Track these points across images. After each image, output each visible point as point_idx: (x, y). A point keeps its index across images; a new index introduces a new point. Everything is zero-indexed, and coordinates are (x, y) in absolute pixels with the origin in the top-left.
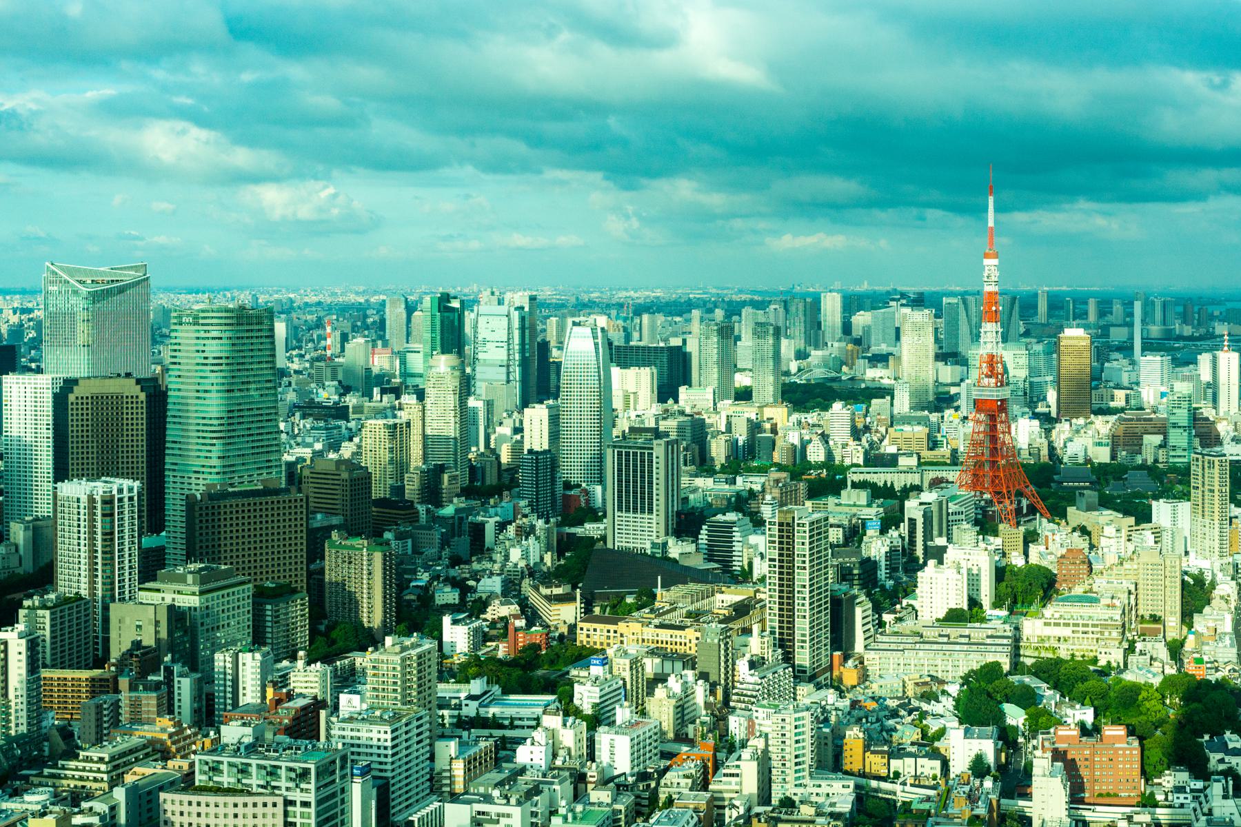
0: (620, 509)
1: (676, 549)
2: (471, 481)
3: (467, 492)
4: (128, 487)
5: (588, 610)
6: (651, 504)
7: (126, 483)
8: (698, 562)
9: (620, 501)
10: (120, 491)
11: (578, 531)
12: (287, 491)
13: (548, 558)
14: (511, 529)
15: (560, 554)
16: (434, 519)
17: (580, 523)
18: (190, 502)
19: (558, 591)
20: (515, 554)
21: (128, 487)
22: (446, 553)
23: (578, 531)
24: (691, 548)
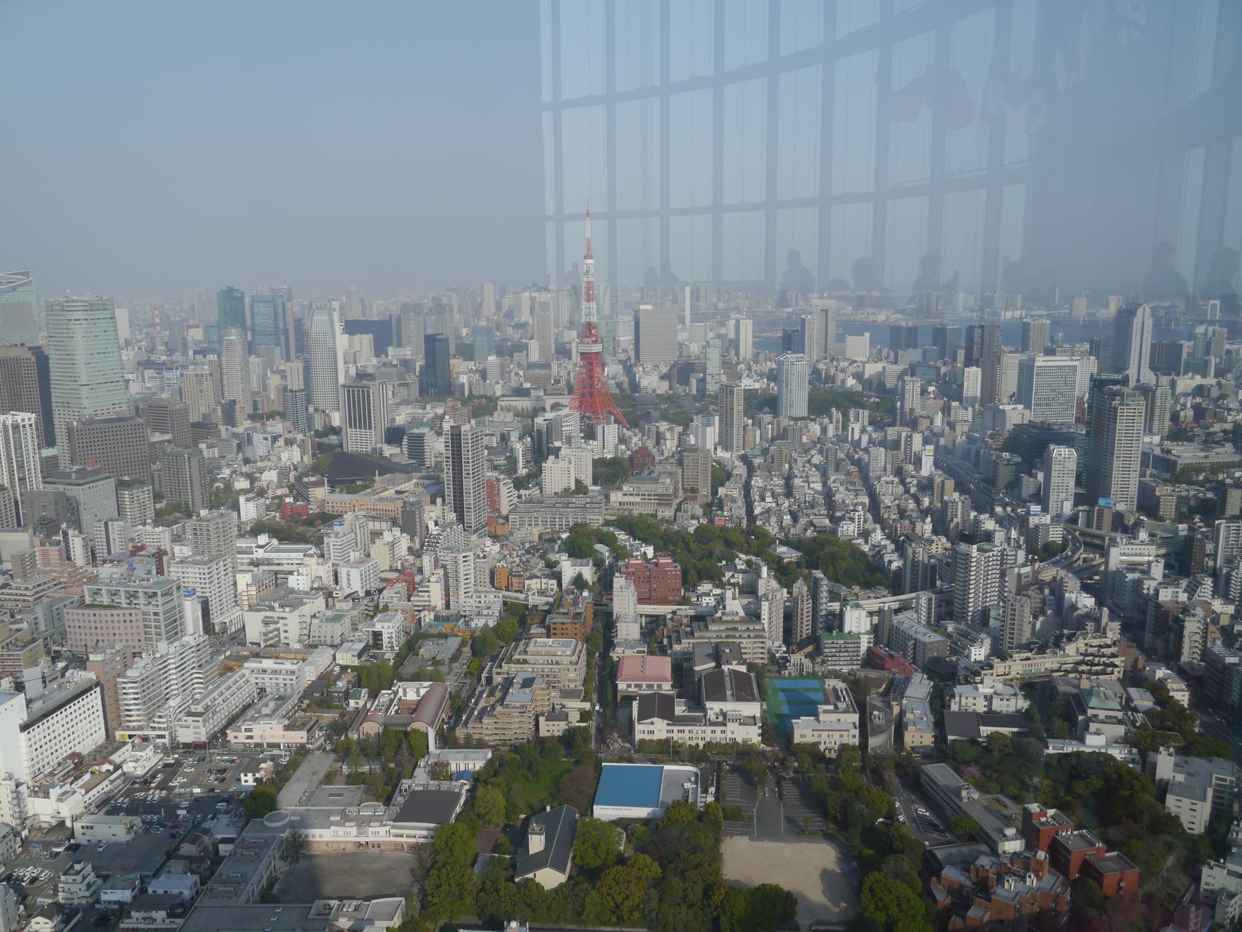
1: (388, 450)
2: (255, 409)
3: (253, 417)
4: (27, 418)
7: (27, 415)
8: (405, 460)
10: (23, 420)
11: (325, 440)
12: (132, 418)
13: (306, 459)
14: (281, 441)
15: (314, 455)
16: (235, 435)
18: (70, 430)
19: (313, 479)
20: (284, 456)
21: (27, 418)
22: (240, 457)
23: (325, 440)
24: (397, 450)
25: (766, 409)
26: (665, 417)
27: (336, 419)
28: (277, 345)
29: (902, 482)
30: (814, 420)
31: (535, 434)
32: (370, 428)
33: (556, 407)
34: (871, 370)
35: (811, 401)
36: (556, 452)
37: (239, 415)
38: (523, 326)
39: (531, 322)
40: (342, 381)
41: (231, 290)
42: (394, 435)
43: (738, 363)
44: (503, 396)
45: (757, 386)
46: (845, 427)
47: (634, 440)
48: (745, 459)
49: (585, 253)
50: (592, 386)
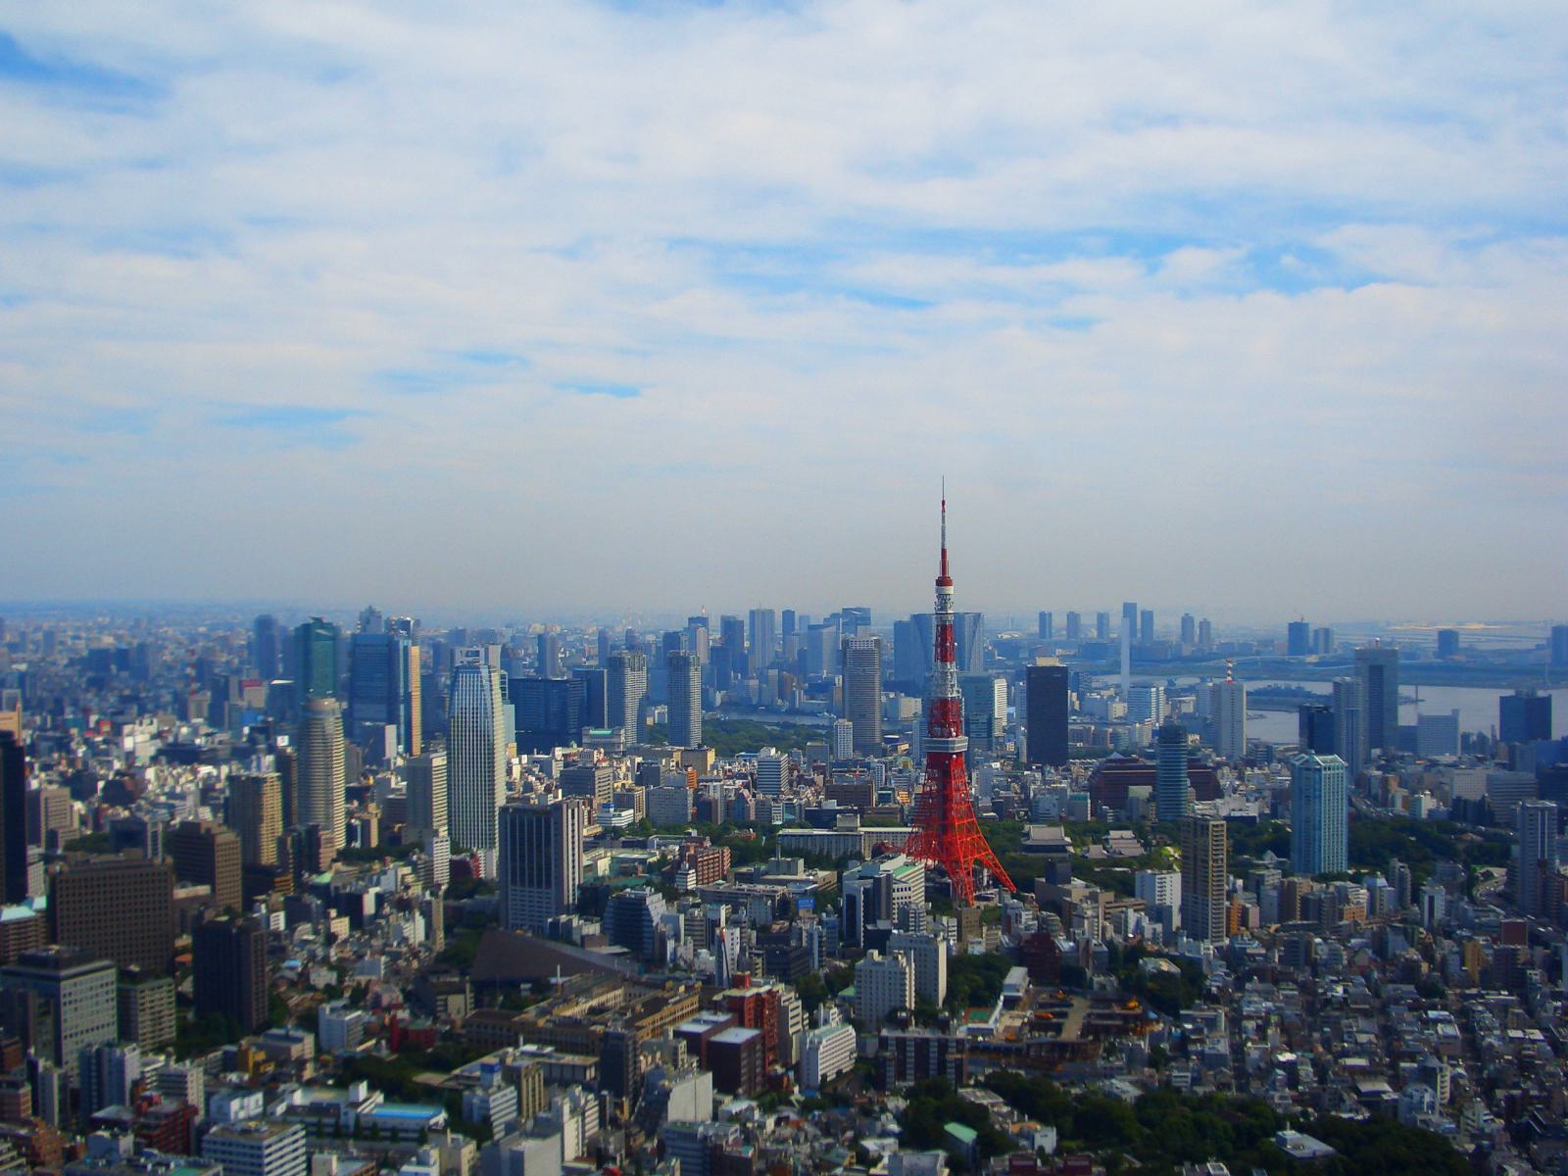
0: (514, 882)
5: (478, 1003)
6: (548, 876)
9: (514, 873)
17: (470, 895)
24: (593, 929)
25: (1270, 857)
26: (1082, 868)
27: (488, 863)
28: (391, 722)
29: (1525, 1001)
30: (1356, 879)
31: (842, 902)
32: (548, 885)
33: (880, 852)
34: (1471, 784)
35: (1350, 844)
36: (880, 940)
37: (326, 854)
38: (822, 688)
39: (839, 680)
40: (501, 800)
41: (318, 621)
42: (593, 899)
43: (1219, 766)
44: (788, 824)
45: (1253, 810)
46: (1416, 899)
47: (1026, 916)
48: (1233, 958)
49: (938, 574)
50: (946, 814)
